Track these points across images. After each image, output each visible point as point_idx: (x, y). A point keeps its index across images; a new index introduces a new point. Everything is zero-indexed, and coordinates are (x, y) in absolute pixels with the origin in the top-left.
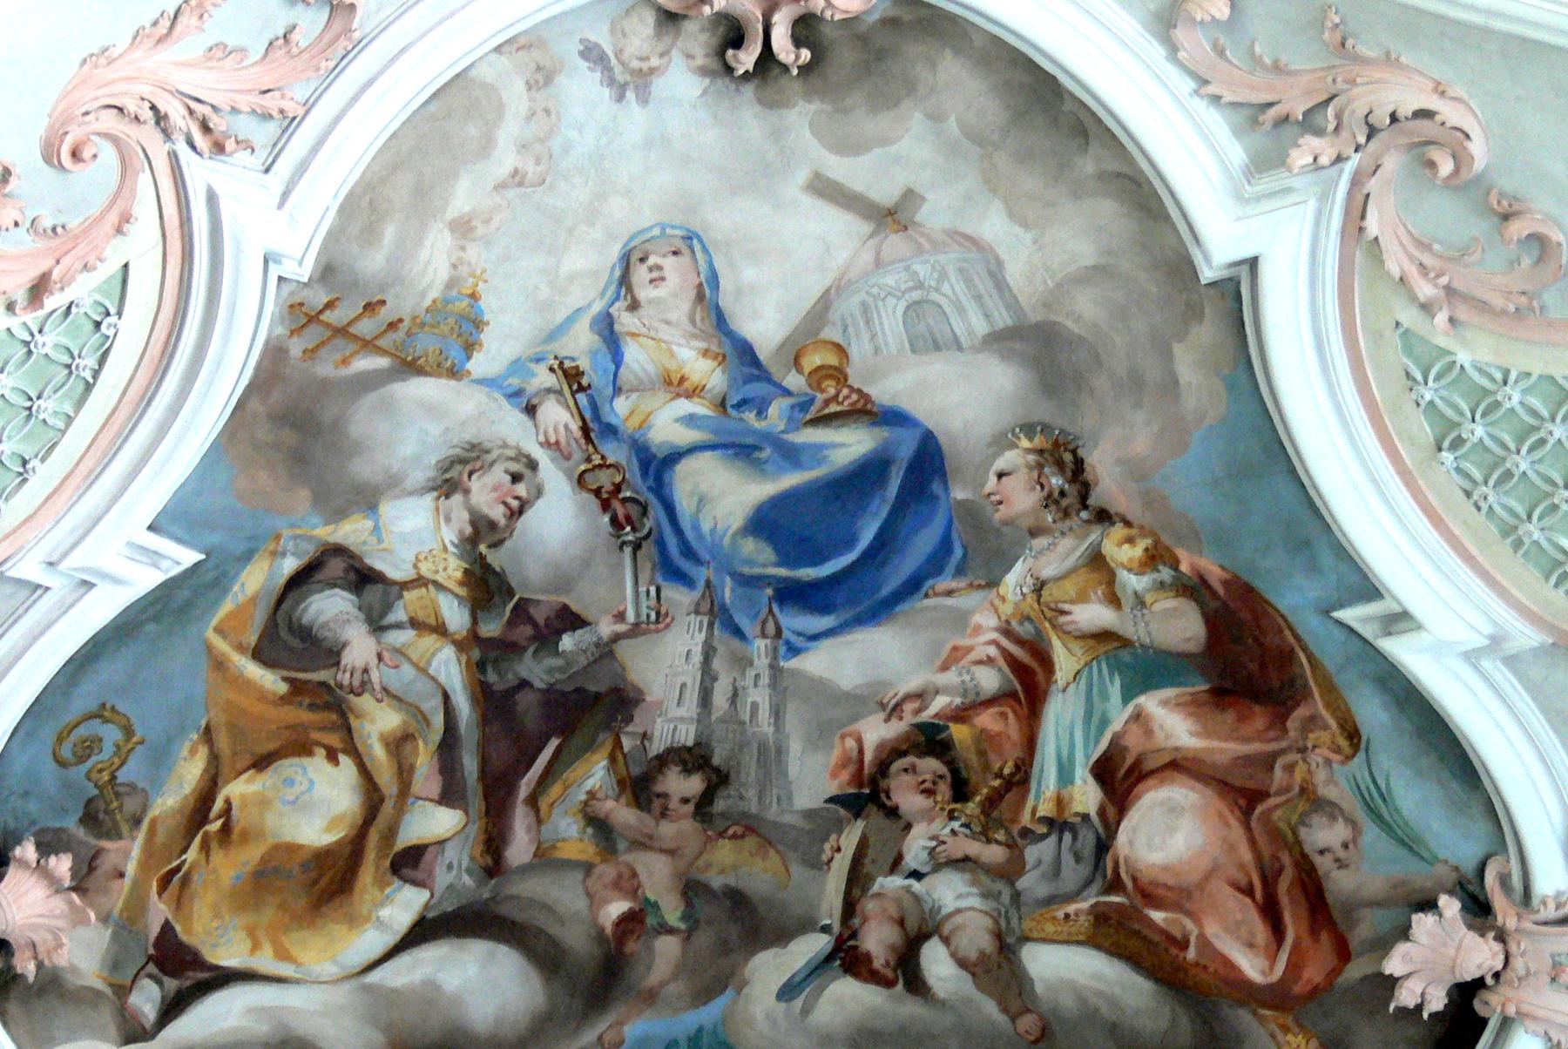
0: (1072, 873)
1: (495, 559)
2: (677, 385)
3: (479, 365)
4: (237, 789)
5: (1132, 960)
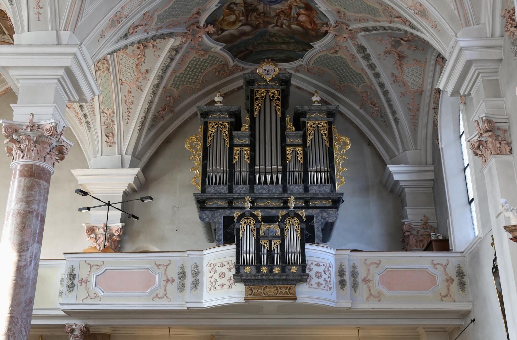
0: (295, 21)
4: (226, 18)
5: (300, 27)
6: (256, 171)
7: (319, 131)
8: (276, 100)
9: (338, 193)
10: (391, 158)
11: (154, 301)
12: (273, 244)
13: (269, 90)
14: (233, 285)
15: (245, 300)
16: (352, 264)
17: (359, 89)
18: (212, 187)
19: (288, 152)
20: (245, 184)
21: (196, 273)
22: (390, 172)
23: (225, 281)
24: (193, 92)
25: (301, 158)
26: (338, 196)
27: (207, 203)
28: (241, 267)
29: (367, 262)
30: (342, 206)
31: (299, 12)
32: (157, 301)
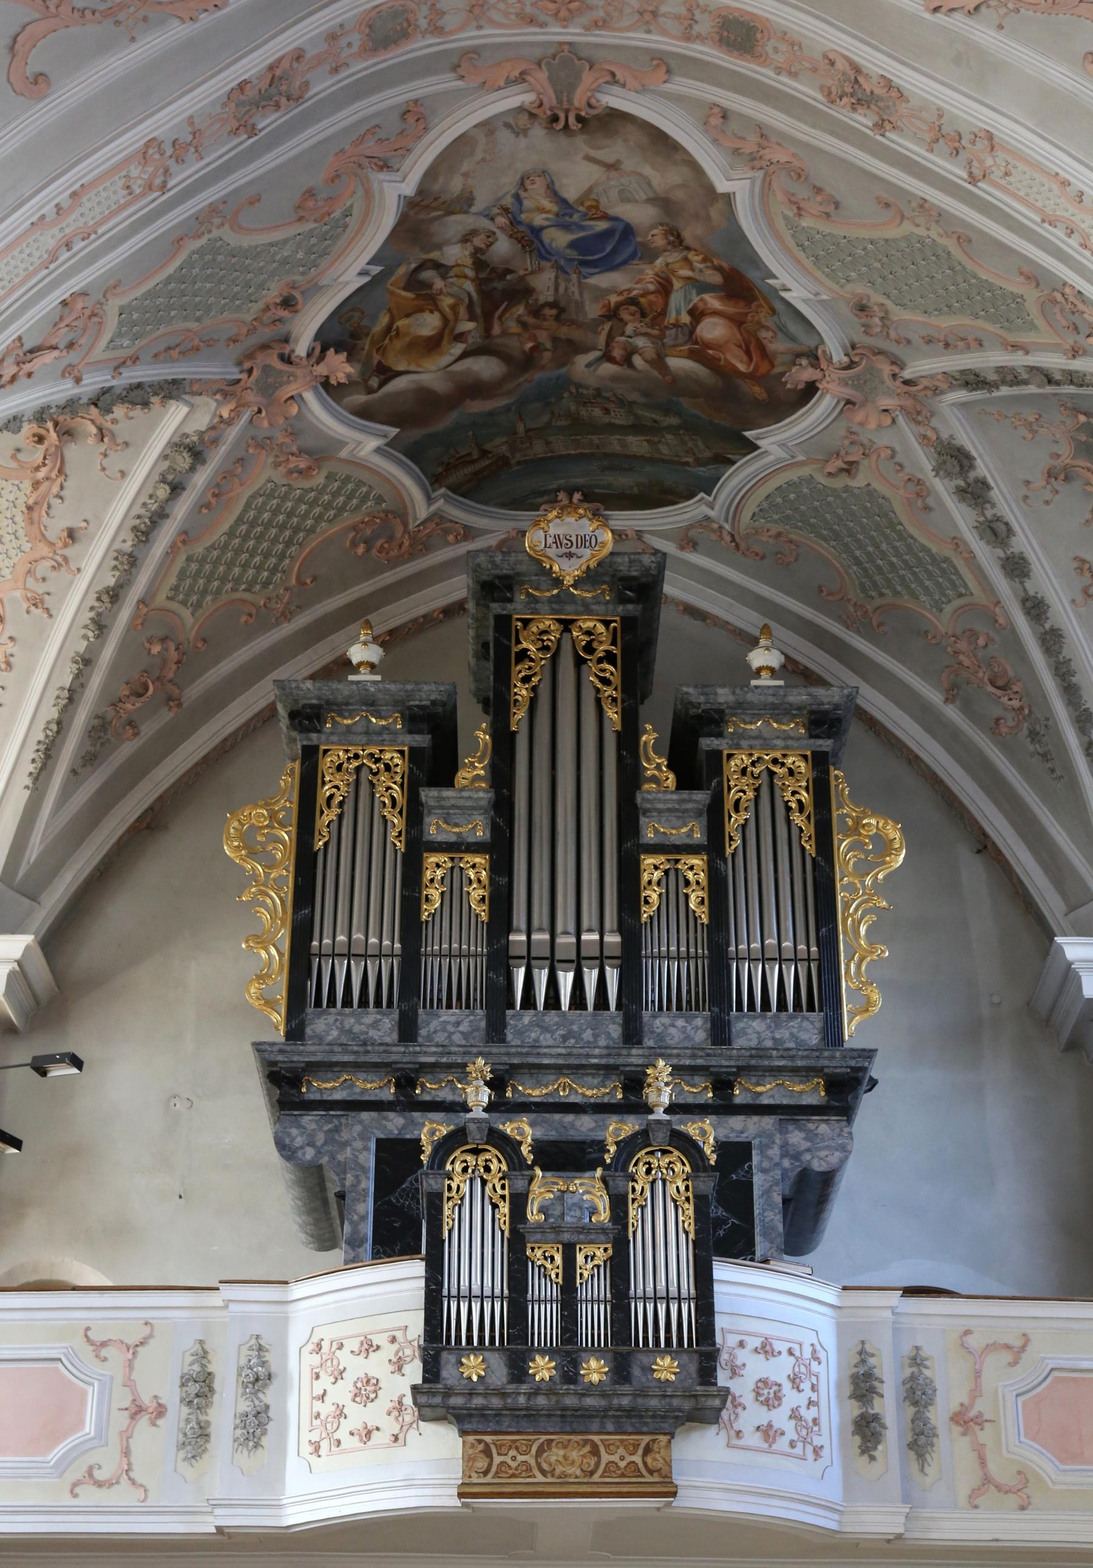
0: (681, 339)
1: (483, 258)
2: (542, 210)
3: (473, 209)
4: (401, 323)
6: (513, 952)
7: (778, 792)
8: (600, 661)
9: (853, 1050)
10: (1071, 909)
11: (75, 1496)
12: (580, 1258)
13: (573, 621)
14: (412, 1434)
15: (461, 1495)
16: (907, 1350)
17: (943, 622)
18: (331, 1019)
19: (645, 877)
20: (468, 1007)
21: (257, 1380)
22: (1069, 964)
23: (376, 1413)
24: (263, 621)
25: (702, 902)
26: (853, 1063)
27: (309, 1082)
28: (445, 1355)
29: (973, 1341)
30: (867, 1105)
31: (701, 305)
32: (89, 1496)
